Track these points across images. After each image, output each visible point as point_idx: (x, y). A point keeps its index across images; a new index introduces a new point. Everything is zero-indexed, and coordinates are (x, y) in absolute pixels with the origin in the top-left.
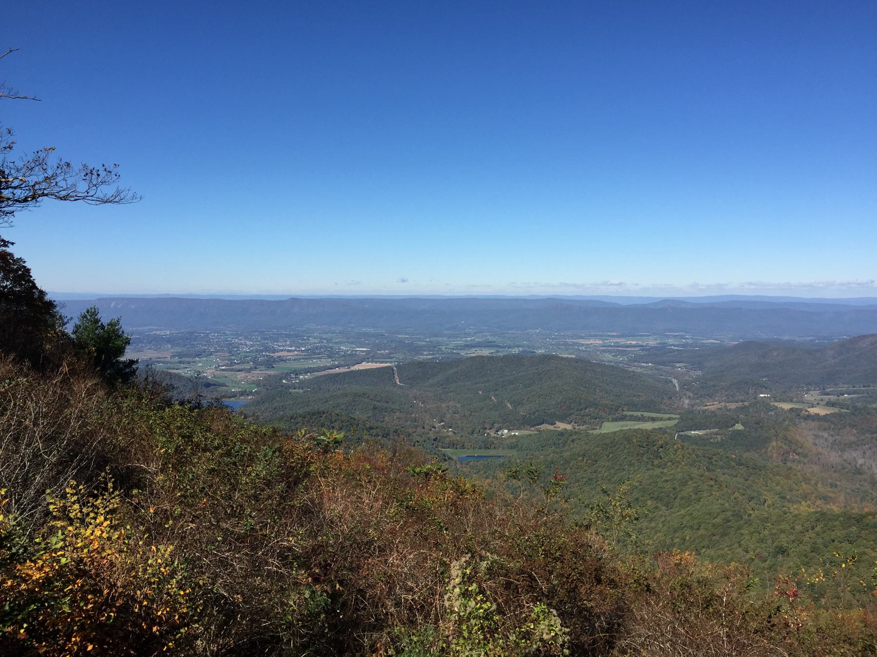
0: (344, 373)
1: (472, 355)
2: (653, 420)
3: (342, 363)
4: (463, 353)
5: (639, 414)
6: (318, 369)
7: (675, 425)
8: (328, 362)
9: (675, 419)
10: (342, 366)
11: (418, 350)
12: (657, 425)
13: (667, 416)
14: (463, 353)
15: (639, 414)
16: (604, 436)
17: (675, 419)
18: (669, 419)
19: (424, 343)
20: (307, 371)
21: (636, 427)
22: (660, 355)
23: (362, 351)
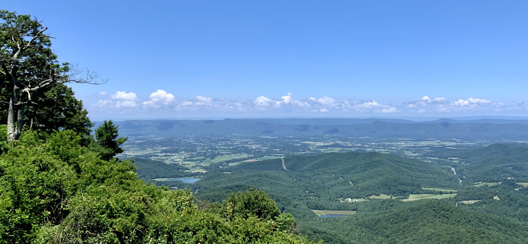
0: (254, 162)
1: (328, 152)
2: (441, 193)
3: (253, 156)
4: (322, 150)
5: (432, 189)
6: (244, 159)
7: (455, 197)
8: (245, 156)
9: (454, 193)
10: (253, 158)
11: (296, 149)
12: (444, 196)
13: (449, 191)
14: (322, 150)
15: (432, 189)
16: (411, 202)
17: (454, 193)
18: (451, 193)
20: (234, 161)
21: (431, 197)
22: (440, 152)
23: (264, 149)
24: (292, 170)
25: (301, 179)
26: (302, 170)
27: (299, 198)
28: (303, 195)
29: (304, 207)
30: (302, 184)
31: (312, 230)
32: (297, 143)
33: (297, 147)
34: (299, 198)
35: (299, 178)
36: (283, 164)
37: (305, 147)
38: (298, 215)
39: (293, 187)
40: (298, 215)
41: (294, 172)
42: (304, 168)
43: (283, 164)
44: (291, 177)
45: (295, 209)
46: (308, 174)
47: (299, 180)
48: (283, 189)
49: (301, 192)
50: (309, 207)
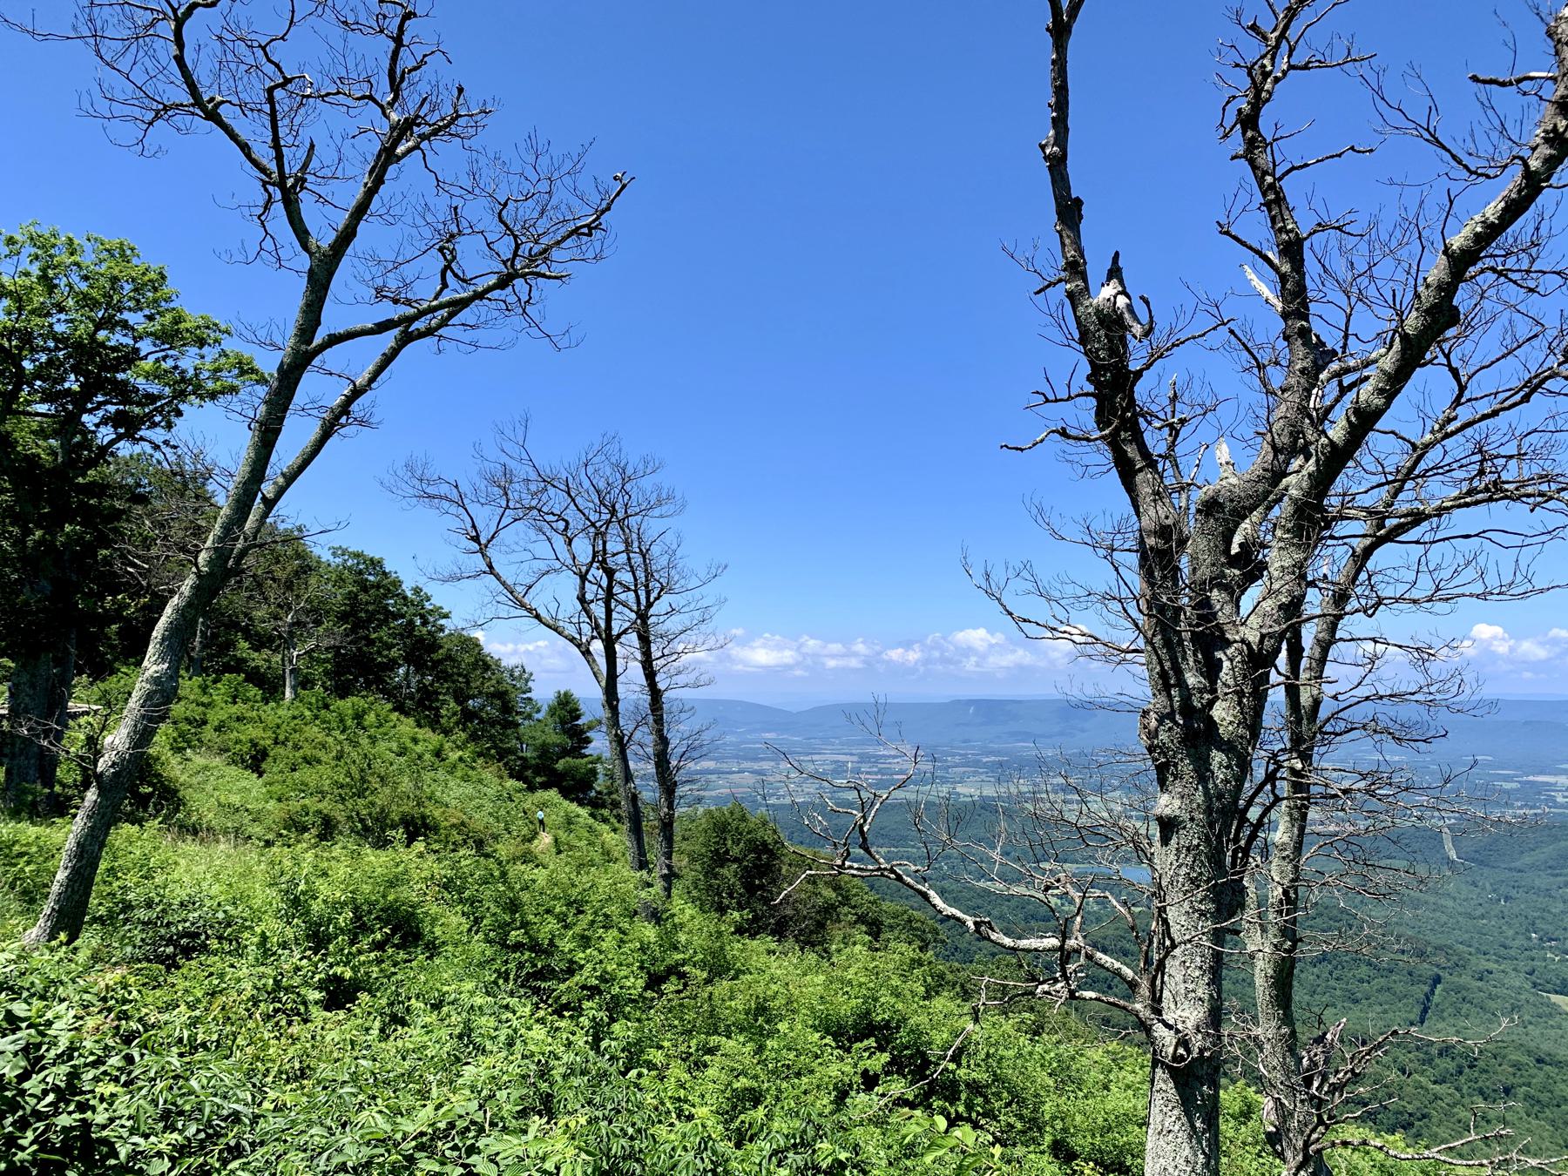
11: (1507, 799)
19: (1514, 785)
24: (1481, 863)
25: (1513, 893)
26: (1518, 864)
27: (1502, 951)
28: (1517, 943)
29: (1517, 981)
30: (1516, 910)
31: (1529, 1053)
32: (1507, 779)
33: (1507, 792)
34: (1502, 951)
35: (1503, 890)
36: (1448, 845)
37: (1534, 792)
38: (1492, 1005)
39: (1483, 917)
40: (1492, 1005)
41: (1486, 871)
42: (1528, 859)
43: (1448, 845)
44: (1474, 884)
45: (1480, 984)
46: (1542, 880)
47: (1507, 899)
48: (1444, 918)
49: (1511, 933)
50: (1535, 985)
